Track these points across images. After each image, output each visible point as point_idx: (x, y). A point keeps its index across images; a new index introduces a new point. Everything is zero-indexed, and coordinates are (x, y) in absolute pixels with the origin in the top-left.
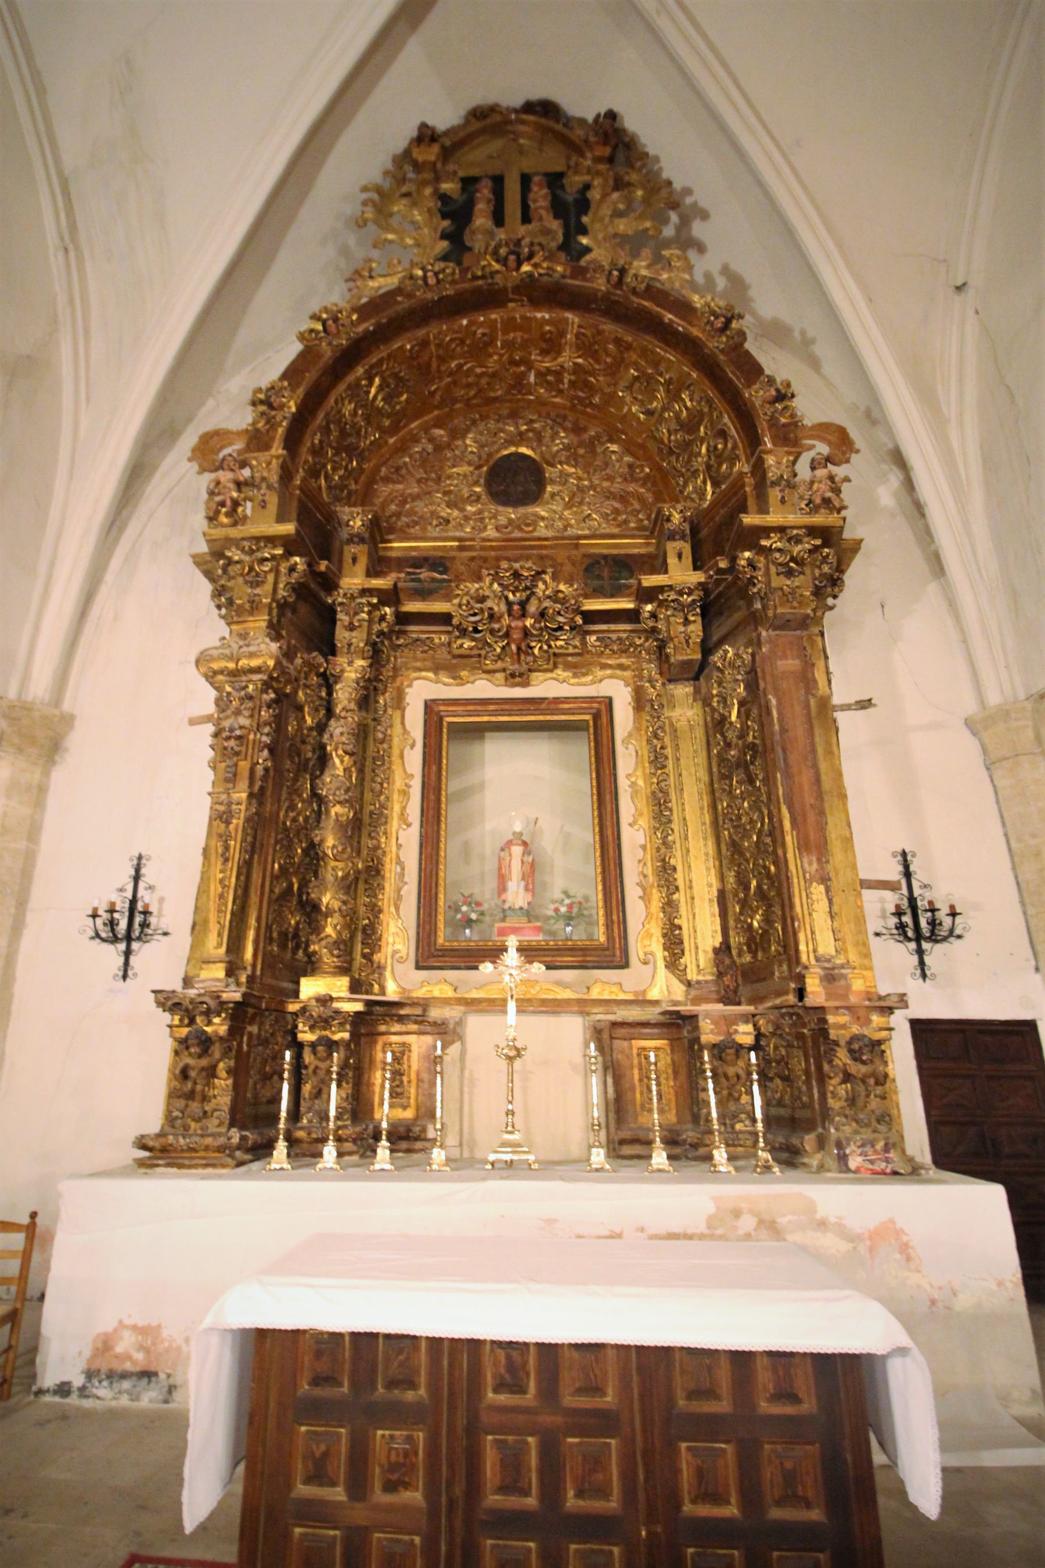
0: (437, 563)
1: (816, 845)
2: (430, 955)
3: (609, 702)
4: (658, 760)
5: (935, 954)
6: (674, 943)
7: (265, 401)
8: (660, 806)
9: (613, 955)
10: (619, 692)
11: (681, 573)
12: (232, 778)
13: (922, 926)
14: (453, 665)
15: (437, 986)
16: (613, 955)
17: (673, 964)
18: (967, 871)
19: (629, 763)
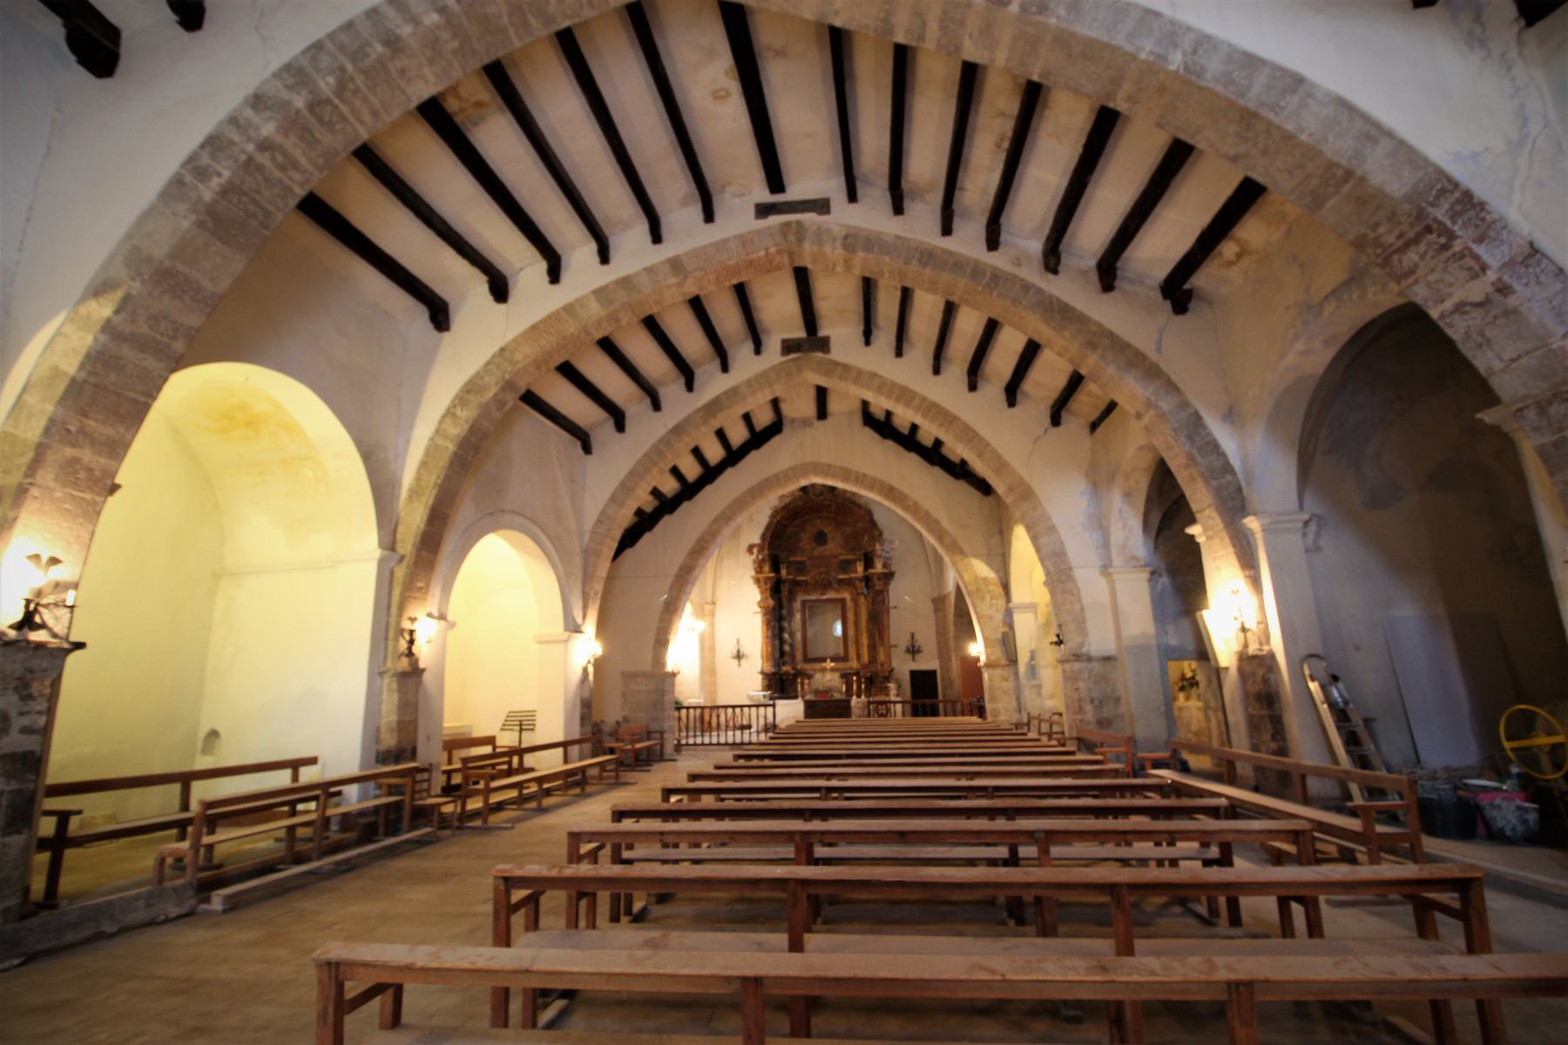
0: (803, 563)
1: (881, 638)
2: (807, 659)
3: (842, 601)
4: (856, 614)
5: (918, 657)
6: (859, 656)
7: (763, 537)
8: (857, 629)
9: (845, 659)
10: (847, 596)
11: (860, 568)
13: (913, 651)
14: (808, 592)
15: (808, 667)
16: (845, 659)
18: (927, 639)
19: (851, 616)
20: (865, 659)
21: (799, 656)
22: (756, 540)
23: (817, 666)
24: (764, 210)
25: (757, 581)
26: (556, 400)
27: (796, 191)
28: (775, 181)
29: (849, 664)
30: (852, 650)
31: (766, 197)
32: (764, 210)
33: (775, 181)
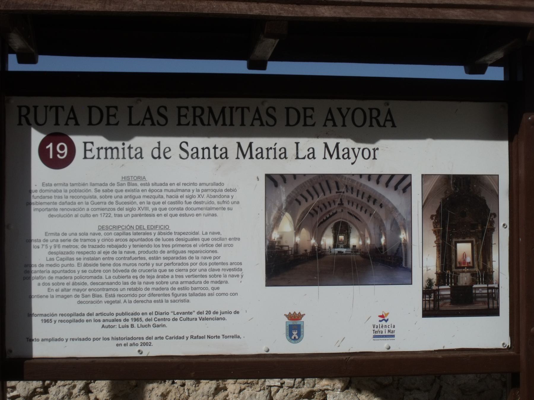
2: (456, 268)
6: (478, 266)
12: (439, 253)
16: (473, 267)
17: (478, 268)
20: (481, 267)
21: (453, 266)
22: (435, 213)
23: (460, 270)
24: (337, 192)
25: (435, 232)
26: (313, 213)
27: (340, 191)
28: (338, 189)
29: (474, 269)
30: (476, 263)
31: (337, 191)
32: (337, 192)
33: (338, 189)
